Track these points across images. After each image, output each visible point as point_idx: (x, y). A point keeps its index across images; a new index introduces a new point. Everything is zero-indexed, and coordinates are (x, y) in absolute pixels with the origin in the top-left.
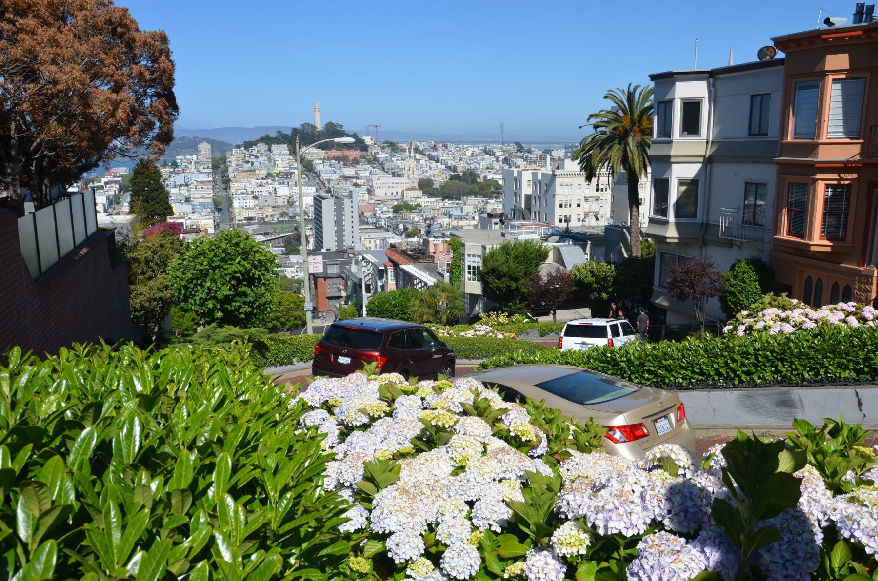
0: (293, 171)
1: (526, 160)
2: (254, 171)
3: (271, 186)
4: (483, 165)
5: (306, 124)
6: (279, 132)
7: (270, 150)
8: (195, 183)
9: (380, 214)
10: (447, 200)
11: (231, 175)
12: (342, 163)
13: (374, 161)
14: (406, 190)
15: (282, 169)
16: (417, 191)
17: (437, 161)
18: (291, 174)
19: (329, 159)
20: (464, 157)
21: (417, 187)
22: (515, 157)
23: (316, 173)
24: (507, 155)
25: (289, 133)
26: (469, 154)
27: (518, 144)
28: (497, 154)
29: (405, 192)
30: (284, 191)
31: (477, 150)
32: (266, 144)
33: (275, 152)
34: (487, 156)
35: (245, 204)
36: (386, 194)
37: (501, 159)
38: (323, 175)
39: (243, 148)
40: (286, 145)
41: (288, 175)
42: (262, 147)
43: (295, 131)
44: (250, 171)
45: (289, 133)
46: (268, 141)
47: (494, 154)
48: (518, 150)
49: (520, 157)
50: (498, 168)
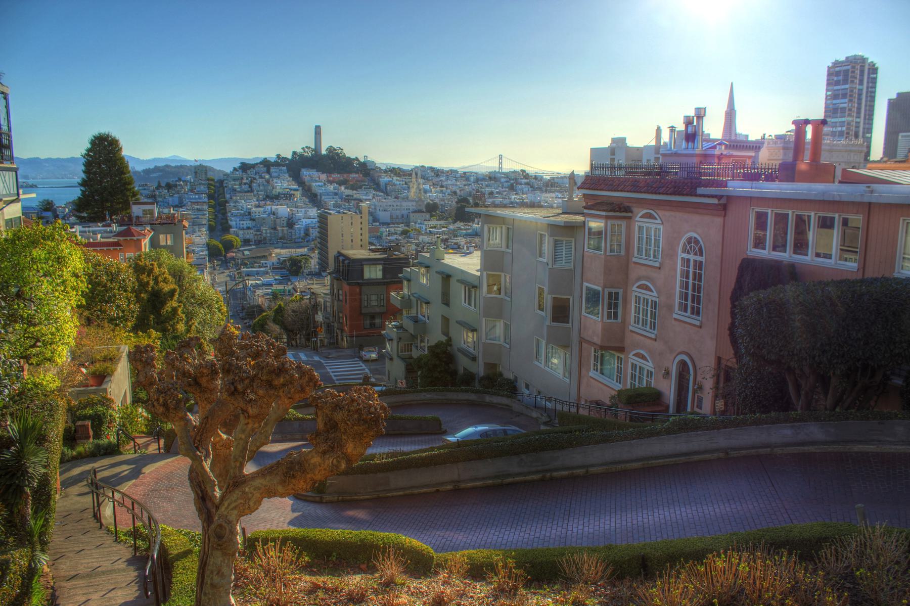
0: (292, 192)
2: (252, 191)
3: (269, 207)
5: (307, 147)
6: (278, 156)
7: (268, 172)
8: (189, 203)
9: (386, 236)
10: (459, 222)
11: (228, 196)
12: (343, 188)
13: (377, 186)
14: (413, 212)
15: (281, 191)
16: (423, 214)
17: (442, 186)
18: (291, 195)
19: (331, 182)
21: (424, 210)
23: (315, 195)
25: (289, 156)
29: (412, 215)
30: (283, 210)
32: (265, 166)
33: (274, 174)
35: (241, 226)
38: (323, 197)
39: (240, 170)
40: (285, 168)
41: (288, 196)
42: (262, 169)
43: (295, 153)
44: (248, 192)
45: (290, 157)
46: (266, 163)
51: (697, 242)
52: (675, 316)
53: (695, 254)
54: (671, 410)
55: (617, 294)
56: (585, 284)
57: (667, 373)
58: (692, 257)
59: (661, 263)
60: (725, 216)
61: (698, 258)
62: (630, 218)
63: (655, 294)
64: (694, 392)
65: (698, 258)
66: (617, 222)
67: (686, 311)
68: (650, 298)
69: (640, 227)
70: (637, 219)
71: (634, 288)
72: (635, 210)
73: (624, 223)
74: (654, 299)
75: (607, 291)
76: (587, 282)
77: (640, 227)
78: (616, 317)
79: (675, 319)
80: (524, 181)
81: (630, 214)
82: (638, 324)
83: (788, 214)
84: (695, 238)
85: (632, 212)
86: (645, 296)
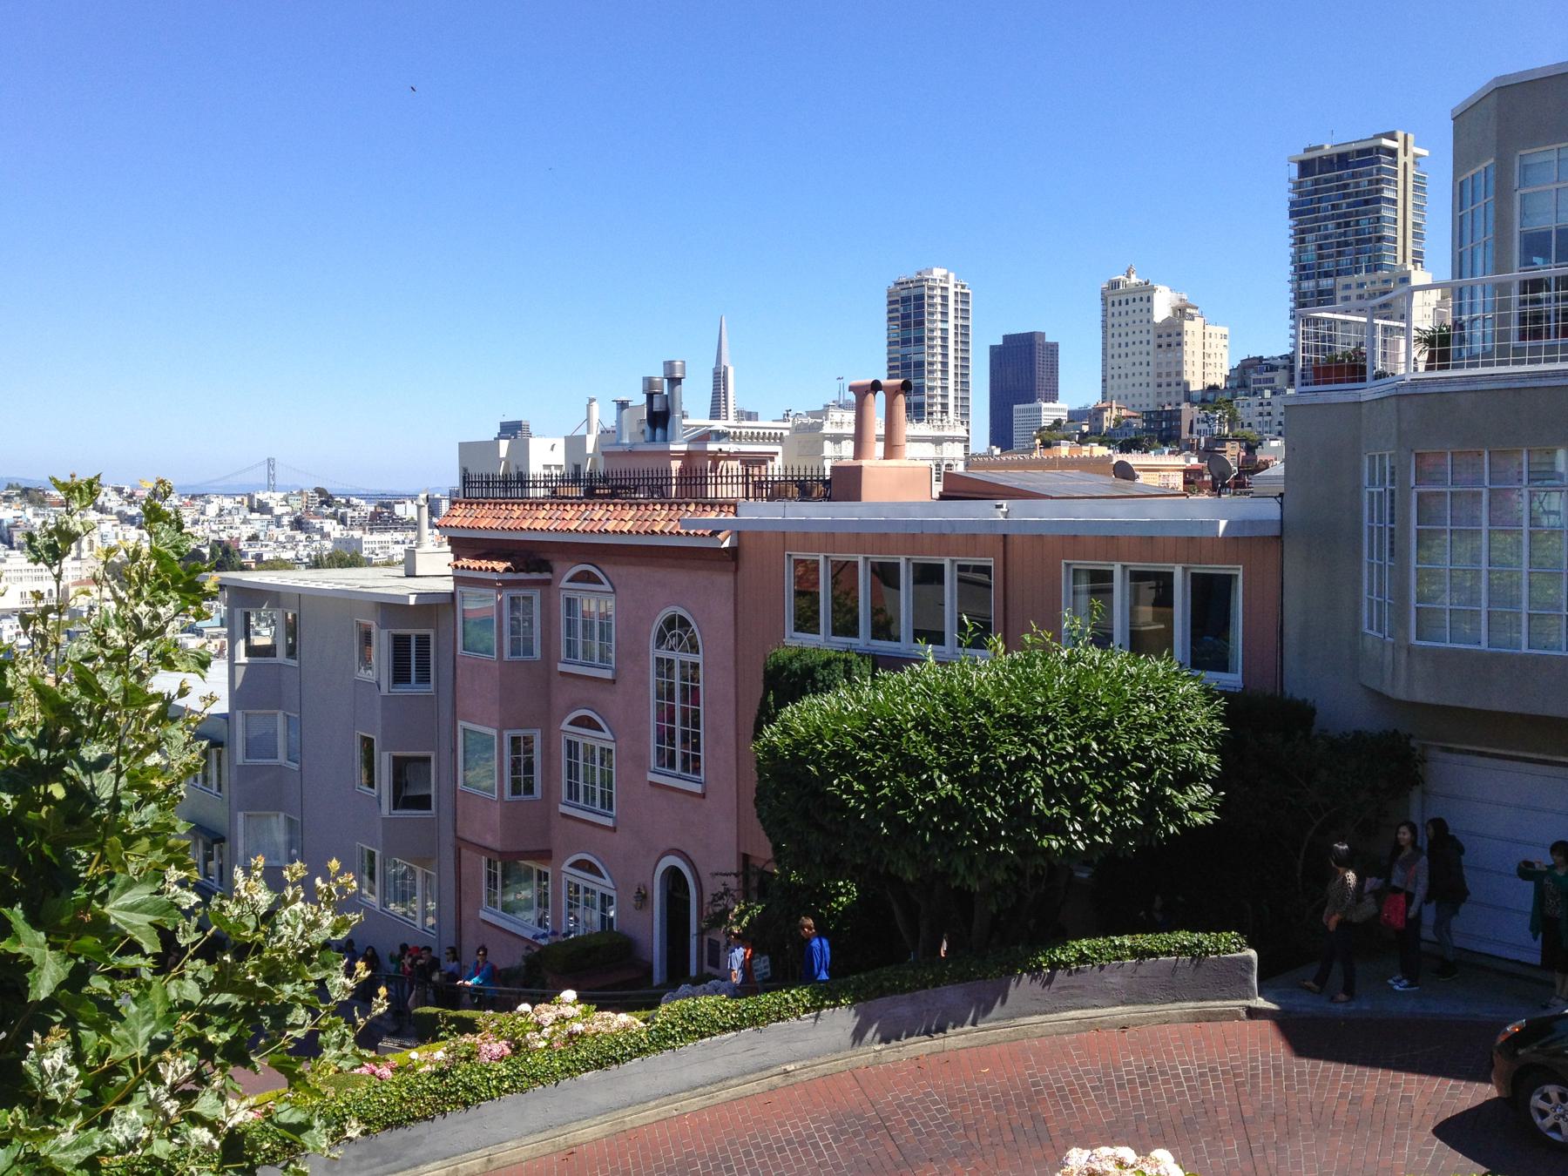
1: (342, 521)
4: (246, 531)
20: (202, 518)
22: (316, 514)
24: (299, 514)
26: (212, 510)
27: (320, 491)
28: (278, 511)
31: (228, 503)
34: (256, 515)
36: (22, 595)
37: (286, 520)
47: (270, 511)
48: (322, 503)
49: (327, 517)
50: (282, 538)
51: (684, 623)
52: (651, 777)
53: (684, 650)
54: (657, 978)
55: (528, 740)
56: (461, 724)
57: (643, 898)
58: (678, 656)
59: (616, 671)
60: (737, 569)
61: (690, 658)
62: (548, 583)
63: (608, 735)
64: (701, 933)
65: (690, 658)
66: (519, 592)
67: (672, 765)
68: (598, 745)
69: (568, 600)
70: (564, 584)
71: (565, 726)
72: (557, 566)
73: (536, 595)
74: (607, 745)
75: (507, 735)
76: (466, 718)
77: (568, 600)
78: (529, 789)
79: (652, 784)
80: (327, 510)
81: (547, 576)
82: (577, 799)
83: (1171, 575)
84: (680, 617)
85: (551, 571)
86: (589, 742)
